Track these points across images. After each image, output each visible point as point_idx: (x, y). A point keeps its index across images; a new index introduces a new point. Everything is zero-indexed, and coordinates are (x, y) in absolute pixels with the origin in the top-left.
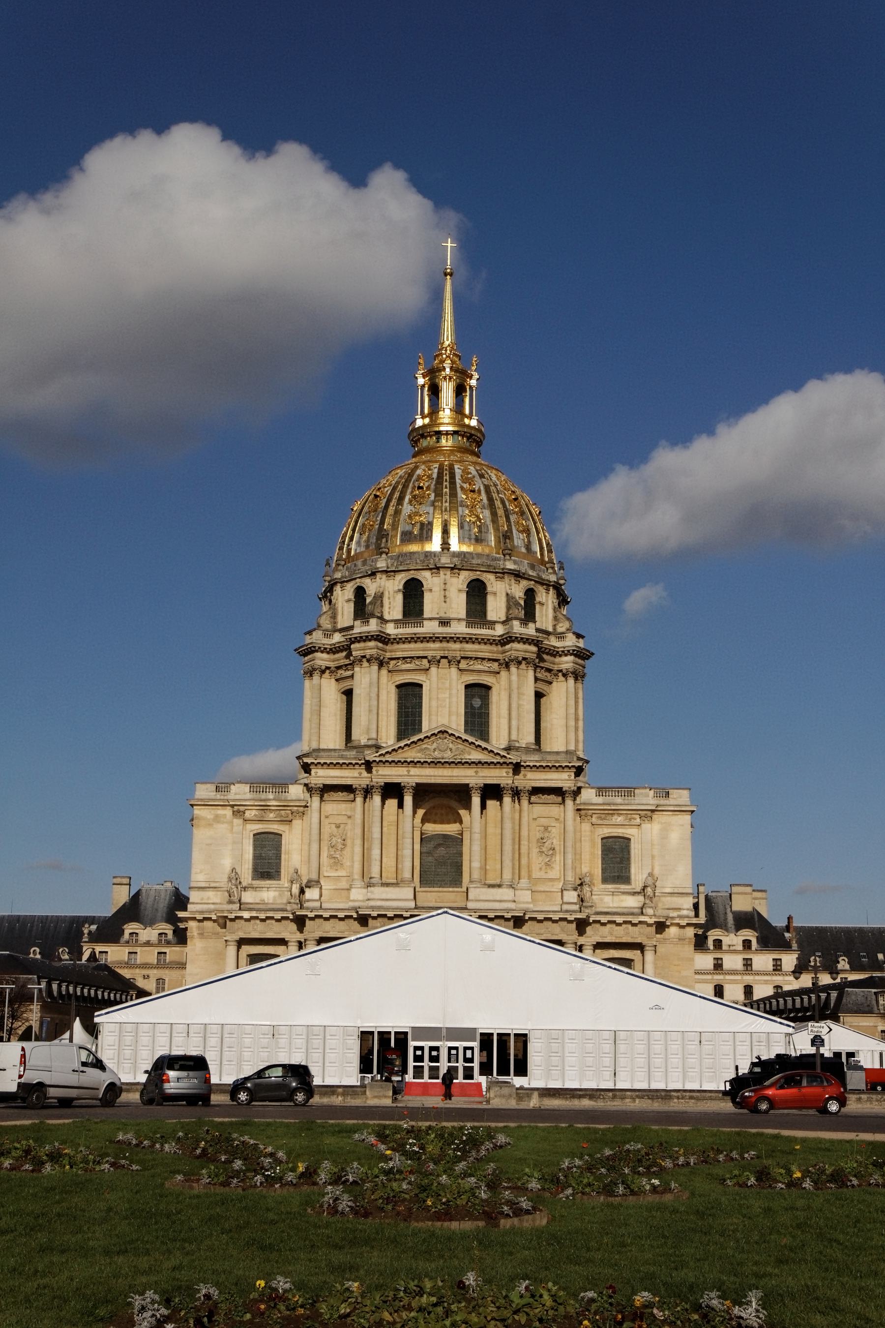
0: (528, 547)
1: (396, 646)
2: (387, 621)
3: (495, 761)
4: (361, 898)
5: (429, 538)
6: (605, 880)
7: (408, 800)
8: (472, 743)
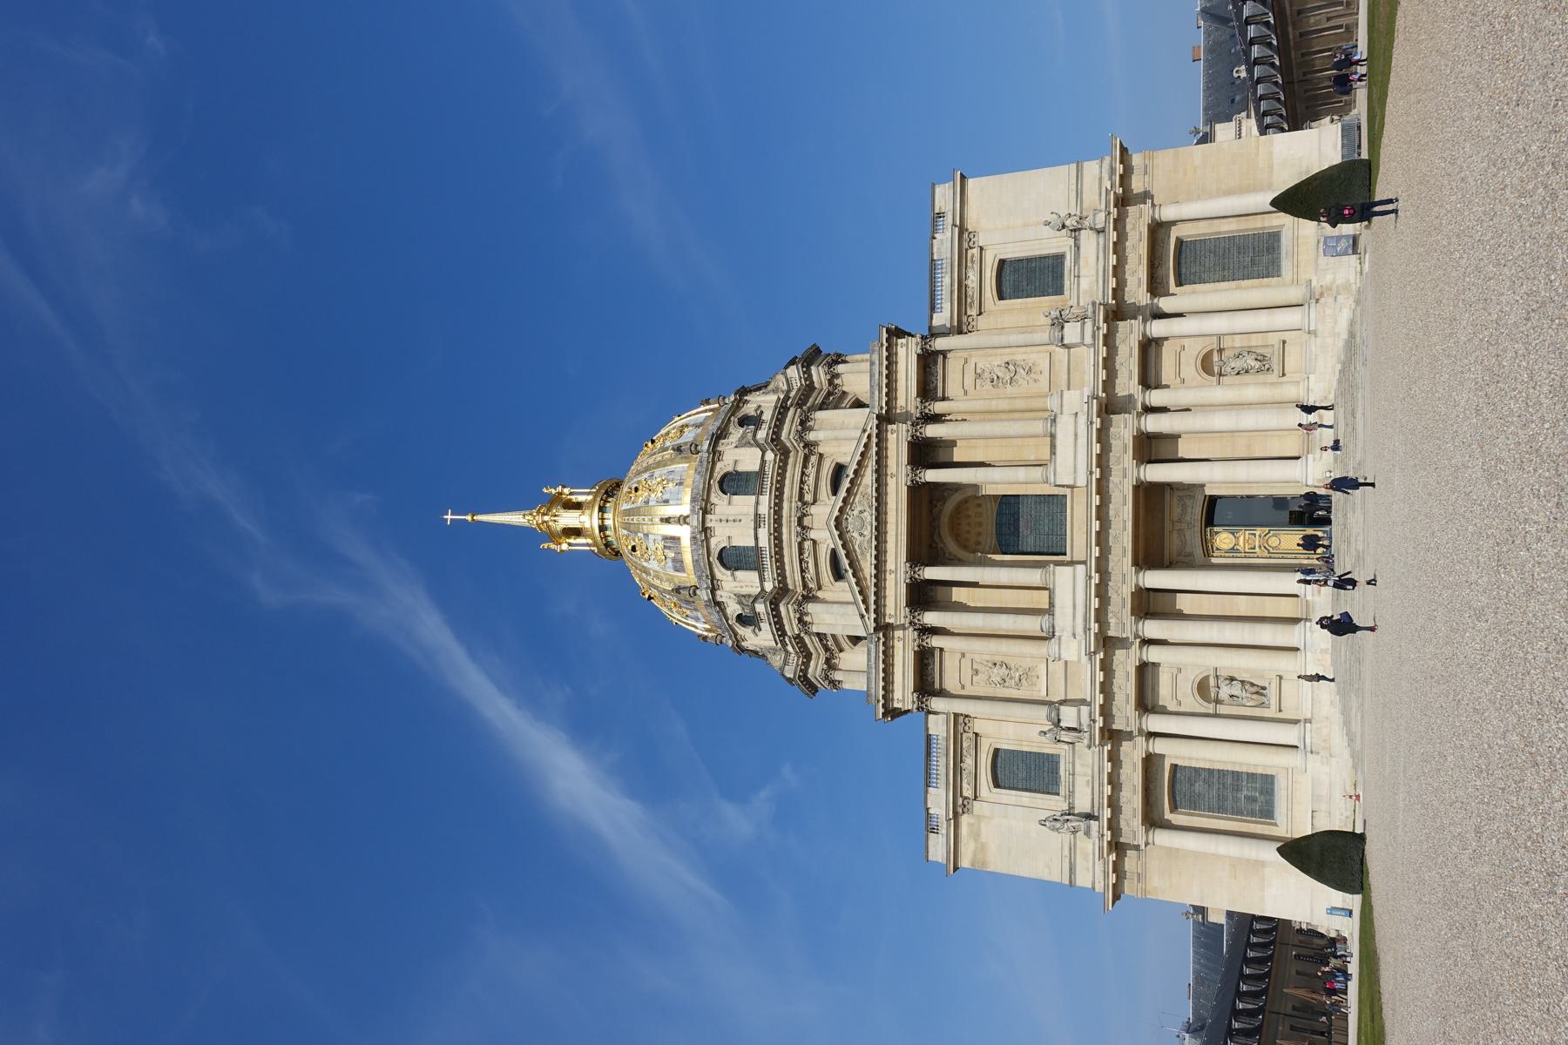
0: (697, 426)
1: (789, 581)
2: (763, 589)
3: (875, 449)
4: (1074, 644)
5: (676, 540)
6: (1059, 291)
7: (931, 573)
8: (852, 482)
